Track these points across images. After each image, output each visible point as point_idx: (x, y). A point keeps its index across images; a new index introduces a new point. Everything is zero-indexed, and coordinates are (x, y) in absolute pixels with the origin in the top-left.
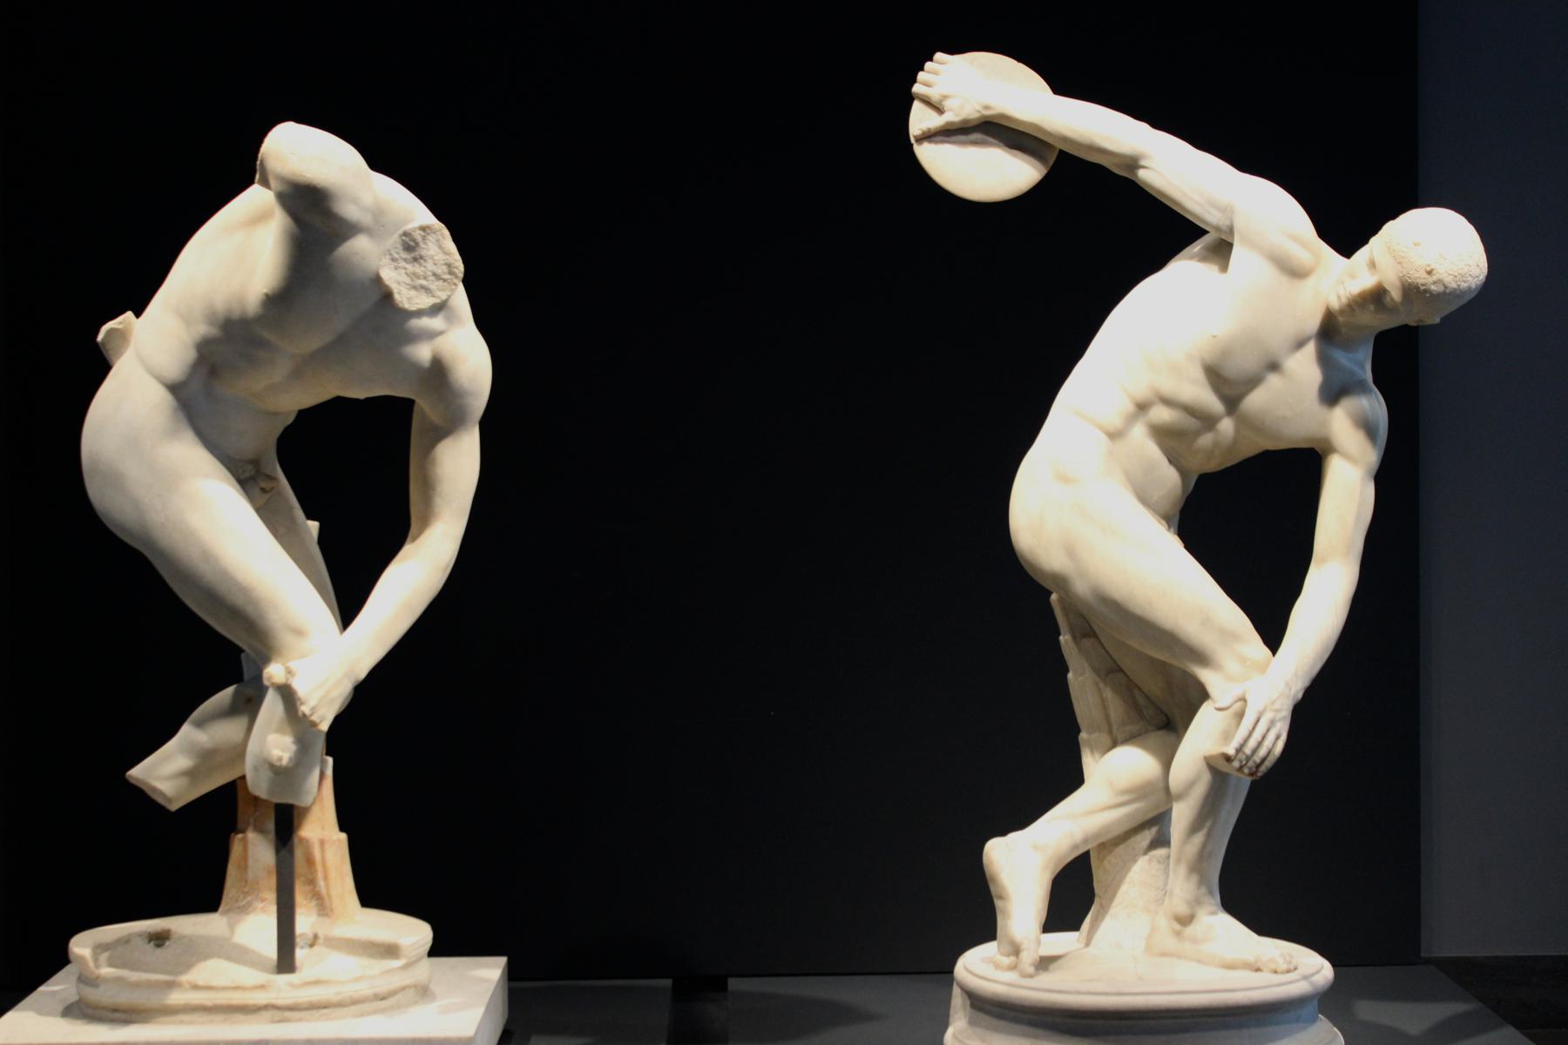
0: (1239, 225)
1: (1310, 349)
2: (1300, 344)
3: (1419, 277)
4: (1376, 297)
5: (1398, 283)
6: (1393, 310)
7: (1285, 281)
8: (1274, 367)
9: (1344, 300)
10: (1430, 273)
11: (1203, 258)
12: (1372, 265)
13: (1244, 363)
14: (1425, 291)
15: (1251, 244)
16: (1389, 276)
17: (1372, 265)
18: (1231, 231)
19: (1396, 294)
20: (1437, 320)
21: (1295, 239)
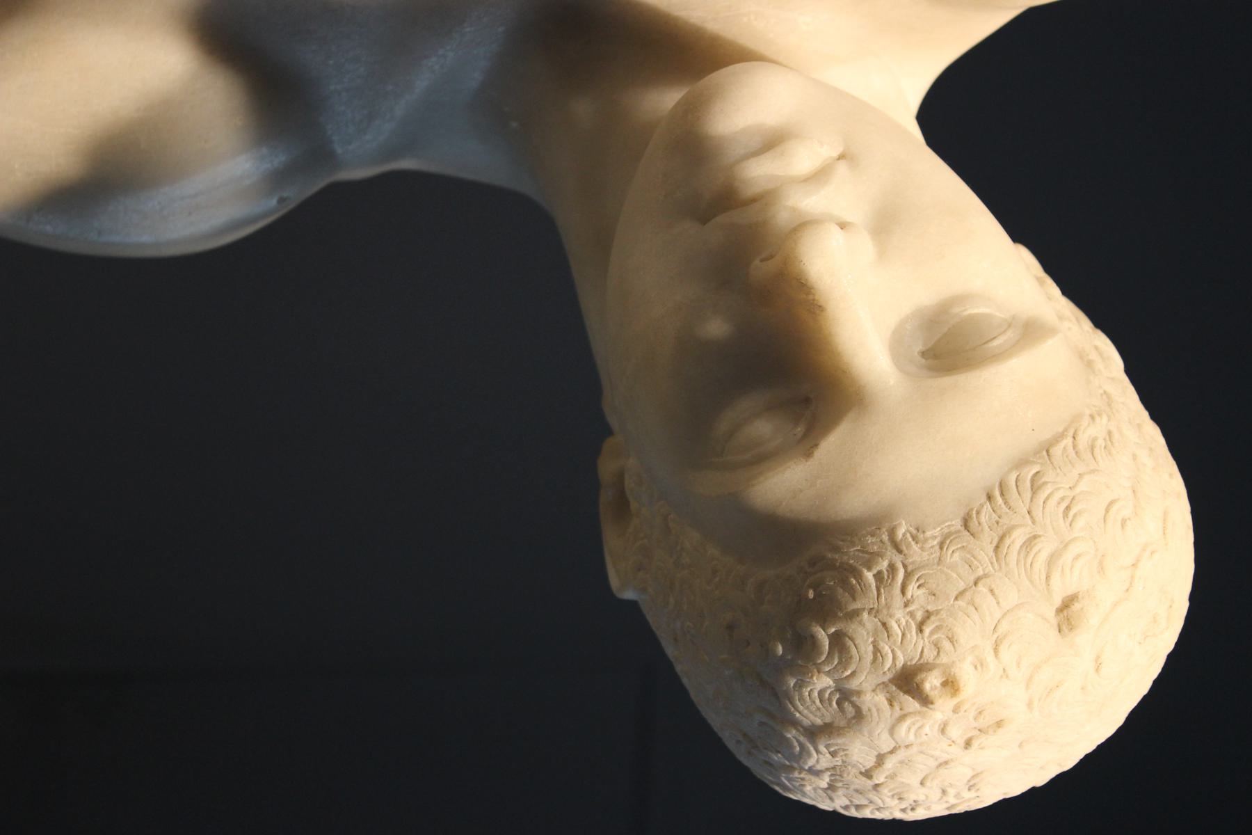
3: (884, 631)
4: (776, 361)
5: (852, 505)
6: (698, 428)
9: (759, 173)
10: (907, 682)
12: (949, 347)
14: (803, 647)
16: (905, 455)
17: (949, 347)
19: (787, 485)
20: (629, 595)
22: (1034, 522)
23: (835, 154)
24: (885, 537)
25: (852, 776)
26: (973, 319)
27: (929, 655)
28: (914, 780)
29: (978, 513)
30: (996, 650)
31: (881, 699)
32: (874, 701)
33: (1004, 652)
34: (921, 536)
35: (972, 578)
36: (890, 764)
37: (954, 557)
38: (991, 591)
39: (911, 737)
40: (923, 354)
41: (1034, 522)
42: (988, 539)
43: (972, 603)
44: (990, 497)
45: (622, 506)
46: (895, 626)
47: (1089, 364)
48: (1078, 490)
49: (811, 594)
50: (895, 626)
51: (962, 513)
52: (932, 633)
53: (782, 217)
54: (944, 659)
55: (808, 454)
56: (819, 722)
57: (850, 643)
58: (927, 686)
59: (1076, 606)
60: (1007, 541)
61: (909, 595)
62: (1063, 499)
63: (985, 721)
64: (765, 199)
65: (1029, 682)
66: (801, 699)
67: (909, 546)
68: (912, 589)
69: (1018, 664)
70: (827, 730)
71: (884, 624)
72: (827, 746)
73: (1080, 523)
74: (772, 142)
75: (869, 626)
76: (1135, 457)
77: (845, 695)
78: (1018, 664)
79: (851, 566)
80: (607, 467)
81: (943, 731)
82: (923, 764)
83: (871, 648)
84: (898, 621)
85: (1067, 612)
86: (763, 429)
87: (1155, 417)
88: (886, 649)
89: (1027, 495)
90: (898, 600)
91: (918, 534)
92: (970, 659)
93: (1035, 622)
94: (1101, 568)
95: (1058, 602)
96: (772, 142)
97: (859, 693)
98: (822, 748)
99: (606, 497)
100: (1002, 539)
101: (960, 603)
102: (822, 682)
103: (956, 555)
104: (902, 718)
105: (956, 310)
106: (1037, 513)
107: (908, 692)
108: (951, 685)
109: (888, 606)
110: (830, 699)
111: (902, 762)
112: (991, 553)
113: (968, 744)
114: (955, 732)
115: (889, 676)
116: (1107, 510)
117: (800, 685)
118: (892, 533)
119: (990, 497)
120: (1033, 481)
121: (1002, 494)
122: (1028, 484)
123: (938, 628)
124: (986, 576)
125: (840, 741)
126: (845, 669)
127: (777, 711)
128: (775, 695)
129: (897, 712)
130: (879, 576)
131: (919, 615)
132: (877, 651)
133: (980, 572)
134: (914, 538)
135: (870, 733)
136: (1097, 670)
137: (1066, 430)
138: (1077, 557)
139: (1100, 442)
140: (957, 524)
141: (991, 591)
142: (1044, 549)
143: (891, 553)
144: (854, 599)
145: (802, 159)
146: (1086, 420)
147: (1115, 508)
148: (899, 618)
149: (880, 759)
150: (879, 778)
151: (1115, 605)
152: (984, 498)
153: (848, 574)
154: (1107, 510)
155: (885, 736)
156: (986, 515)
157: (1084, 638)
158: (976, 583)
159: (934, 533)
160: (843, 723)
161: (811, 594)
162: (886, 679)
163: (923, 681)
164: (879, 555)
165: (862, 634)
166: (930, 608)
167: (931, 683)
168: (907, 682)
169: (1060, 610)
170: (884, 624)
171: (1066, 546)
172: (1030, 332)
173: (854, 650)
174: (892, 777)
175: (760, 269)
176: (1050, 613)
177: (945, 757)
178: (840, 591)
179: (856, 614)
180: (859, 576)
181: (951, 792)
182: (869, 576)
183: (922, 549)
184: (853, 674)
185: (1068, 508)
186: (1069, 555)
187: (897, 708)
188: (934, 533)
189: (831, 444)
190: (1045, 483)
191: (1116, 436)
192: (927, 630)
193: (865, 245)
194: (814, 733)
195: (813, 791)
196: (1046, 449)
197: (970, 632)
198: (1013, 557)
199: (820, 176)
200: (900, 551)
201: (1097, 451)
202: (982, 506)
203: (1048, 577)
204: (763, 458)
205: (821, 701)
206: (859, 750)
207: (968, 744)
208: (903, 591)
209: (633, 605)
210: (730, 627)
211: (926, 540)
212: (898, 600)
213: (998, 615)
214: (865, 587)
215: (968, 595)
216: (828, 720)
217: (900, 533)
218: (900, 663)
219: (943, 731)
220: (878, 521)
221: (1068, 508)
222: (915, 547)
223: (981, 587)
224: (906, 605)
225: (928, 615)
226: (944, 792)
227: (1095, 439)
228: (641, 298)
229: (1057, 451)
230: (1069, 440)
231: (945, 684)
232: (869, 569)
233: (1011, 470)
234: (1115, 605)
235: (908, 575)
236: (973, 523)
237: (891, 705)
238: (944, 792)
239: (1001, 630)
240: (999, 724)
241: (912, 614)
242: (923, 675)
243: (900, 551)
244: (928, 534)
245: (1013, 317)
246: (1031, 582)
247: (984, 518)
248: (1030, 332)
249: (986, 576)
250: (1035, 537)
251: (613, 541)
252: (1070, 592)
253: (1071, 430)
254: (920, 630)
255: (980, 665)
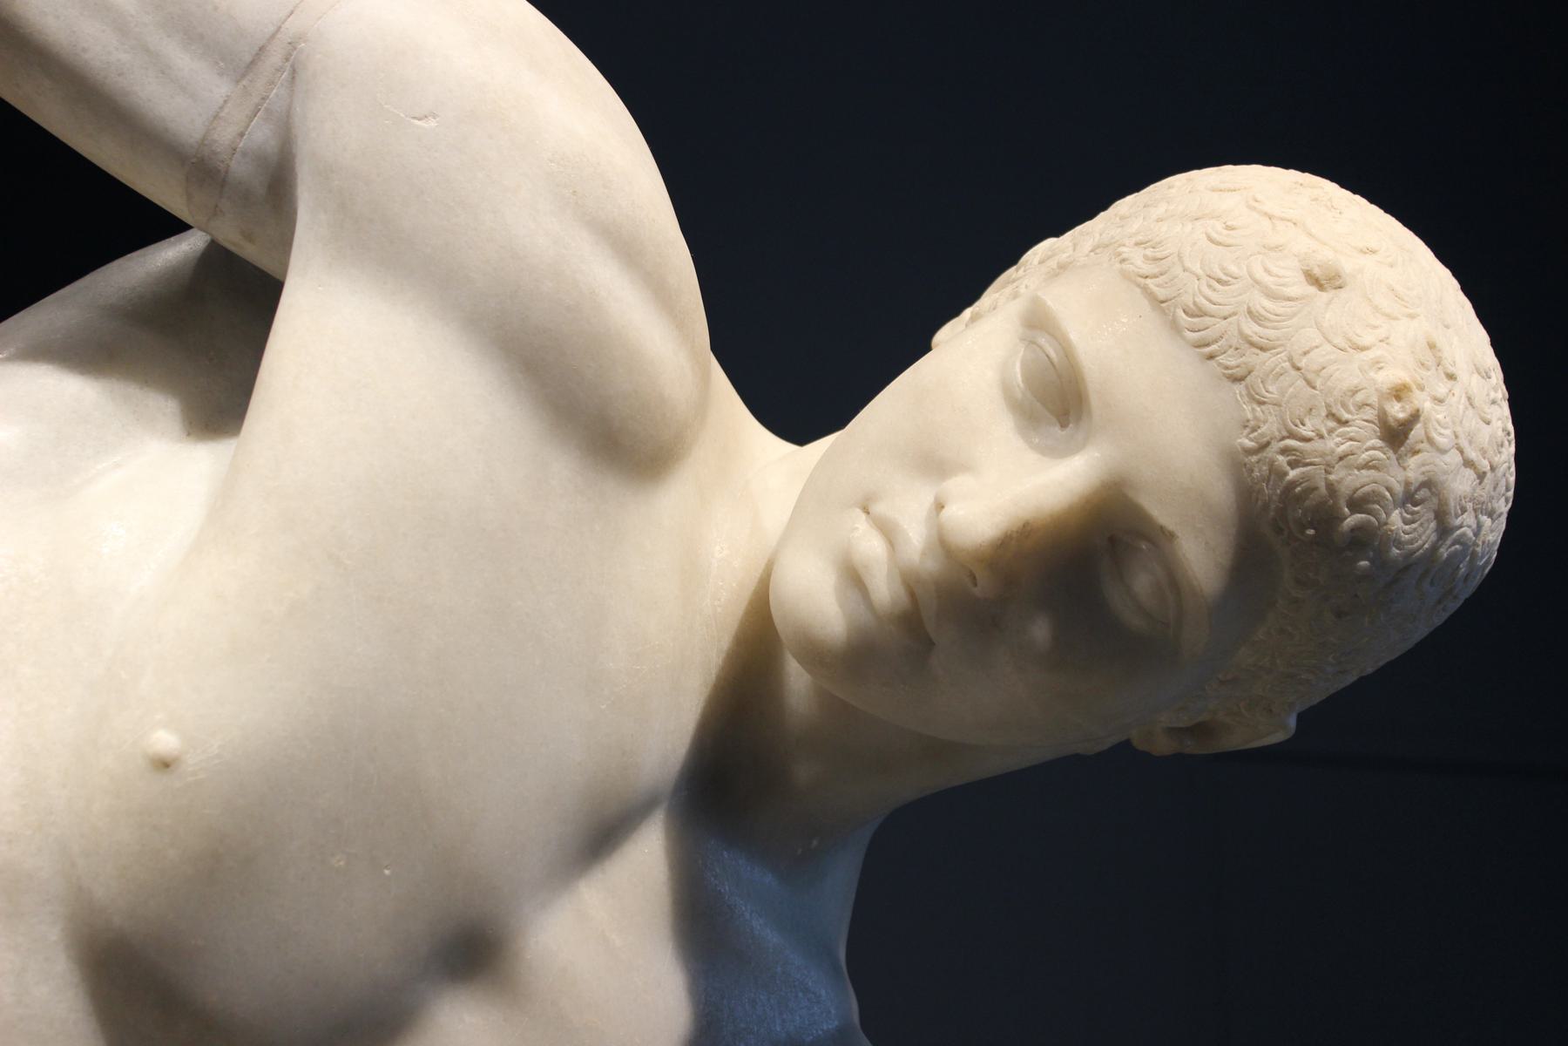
0: (333, 134)
1: (647, 856)
2: (601, 837)
3: (1348, 457)
4: (1076, 570)
5: (1220, 492)
7: (563, 468)
8: (472, 951)
9: (884, 589)
10: (1396, 435)
11: (88, 354)
12: (1057, 400)
13: (344, 924)
14: (1363, 540)
15: (398, 251)
16: (1170, 440)
17: (1057, 400)
18: (274, 189)
19: (1201, 557)
20: (1292, 722)
21: (626, 248)
22: (1235, 314)
23: (864, 516)
24: (1254, 459)
25: (1483, 493)
26: (1028, 379)
27: (1370, 414)
28: (1486, 430)
29: (1227, 368)
30: (1363, 349)
31: (1412, 462)
32: (1413, 469)
33: (1367, 338)
34: (1252, 423)
35: (1294, 373)
36: (1473, 455)
37: (1273, 391)
38: (1305, 353)
39: (1447, 432)
40: (1063, 426)
41: (1235, 314)
42: (1253, 358)
43: (1318, 372)
44: (1211, 357)
45: (1201, 730)
46: (1343, 447)
47: (1063, 267)
48: (1200, 272)
49: (1311, 532)
50: (1343, 447)
51: (1228, 384)
52: (1349, 412)
53: (931, 566)
54: (1374, 400)
55: (1171, 536)
56: (1433, 525)
57: (1359, 493)
58: (1401, 416)
59: (1317, 271)
60: (1255, 339)
61: (1311, 434)
62: (1210, 286)
63: (1431, 362)
64: (911, 583)
65: (1388, 316)
66: (1411, 542)
67: (1262, 435)
68: (1306, 431)
69: (1375, 327)
70: (1441, 516)
71: (1341, 459)
72: (1457, 516)
73: (1233, 269)
74: (853, 577)
75: (1342, 473)
76: (1159, 220)
77: (1409, 498)
78: (1375, 327)
79: (1283, 492)
80: (1163, 746)
81: (1440, 401)
82: (1472, 422)
83: (1364, 472)
84: (1338, 445)
85: (1323, 280)
86: (1143, 583)
87: (1105, 206)
88: (1365, 456)
89: (1207, 320)
90: (1317, 445)
91: (1248, 426)
92: (1372, 374)
93: (1332, 310)
94: (1277, 248)
95: (1313, 290)
96: (853, 577)
97: (1407, 484)
98: (1458, 522)
99: (1191, 747)
100: (1252, 344)
101: (1318, 384)
102: (1396, 519)
103: (1270, 388)
104: (1431, 441)
105: (1019, 396)
106: (1226, 310)
107: (1406, 435)
108: (1399, 393)
109: (1323, 455)
110: (1412, 513)
111: (1470, 443)
112: (1267, 354)
113: (1451, 377)
114: (1442, 389)
115: (1391, 453)
116: (1219, 244)
117: (1399, 543)
118: (1249, 452)
119: (1211, 357)
120: (1193, 316)
121: (1208, 345)
122: (1195, 320)
123: (1344, 405)
124: (1290, 359)
125: (1452, 503)
126: (1384, 497)
127: (1424, 566)
128: (1407, 568)
129: (1425, 446)
130: (1293, 464)
131: (1332, 424)
132: (1367, 466)
133: (1287, 365)
134: (1254, 430)
135: (1445, 473)
136: (1374, 252)
137: (1139, 285)
138: (1267, 271)
139: (1149, 252)
140: (1238, 388)
141: (1305, 353)
142: (1263, 304)
143: (1270, 453)
144: (1316, 488)
145: (870, 547)
146: (1125, 266)
147: (1214, 235)
148: (1335, 444)
149: (1468, 463)
150: (1485, 465)
151: (1310, 234)
152: (1212, 363)
153: (1291, 495)
154: (1219, 244)
155: (1447, 458)
156: (1229, 360)
157: (1347, 265)
158: (1298, 369)
159: (1248, 410)
160: (1435, 500)
161: (1311, 532)
162: (1393, 456)
163: (1396, 420)
164: (1272, 463)
165: (1350, 480)
166: (1324, 414)
167: (1397, 411)
168: (1396, 435)
169: (1321, 287)
170: (1341, 459)
171: (1257, 282)
172: (1037, 322)
173: (1366, 489)
174: (1484, 452)
175: (984, 587)
176: (1324, 296)
177: (1464, 400)
178: (1307, 503)
179: (1332, 488)
180: (1293, 484)
181: (1493, 395)
182: (1293, 474)
183: (1265, 422)
184: (1388, 489)
185: (1219, 281)
186: (1268, 280)
187: (1421, 446)
188: (1248, 410)
189: (1161, 514)
190: (1195, 303)
191: (1140, 238)
192: (1346, 416)
193: (956, 485)
194: (1444, 530)
195: (1493, 532)
196: (1158, 303)
197: (1347, 374)
198: (1271, 333)
199: (888, 531)
200: (1268, 444)
201: (1159, 255)
202: (1220, 364)
203: (1289, 299)
204: (1173, 580)
205: (1413, 522)
206: (1461, 485)
207: (1451, 377)
208: (1308, 440)
209: (1300, 717)
210: (1339, 614)
211: (1256, 418)
212: (1317, 445)
213: (1328, 347)
214: (1305, 478)
215: (1310, 376)
216: (1432, 515)
217: (1249, 444)
218: (1378, 443)
219: (1440, 401)
220: (1238, 465)
221: (1219, 281)
222: (1264, 429)
223: (1302, 363)
224: (1322, 437)
225: (1331, 415)
226: (1494, 402)
227: (1146, 257)
228: (1003, 712)
229: (1161, 293)
230: (1148, 281)
231: (1398, 398)
232: (1286, 474)
233: (1183, 338)
234: (1310, 234)
235: (1292, 435)
236: (1238, 372)
237: (1417, 452)
238: (1494, 402)
239: (1343, 344)
240: (1432, 346)
241: (1331, 431)
242: (1391, 420)
243: (1268, 444)
244: (1250, 416)
245: (1022, 339)
246: (1294, 315)
247: (1232, 362)
248: (1037, 322)
249: (1290, 359)
250: (1250, 312)
251: (1238, 739)
252: (1302, 278)
253: (1139, 281)
254: (1345, 423)
255: (1377, 364)
